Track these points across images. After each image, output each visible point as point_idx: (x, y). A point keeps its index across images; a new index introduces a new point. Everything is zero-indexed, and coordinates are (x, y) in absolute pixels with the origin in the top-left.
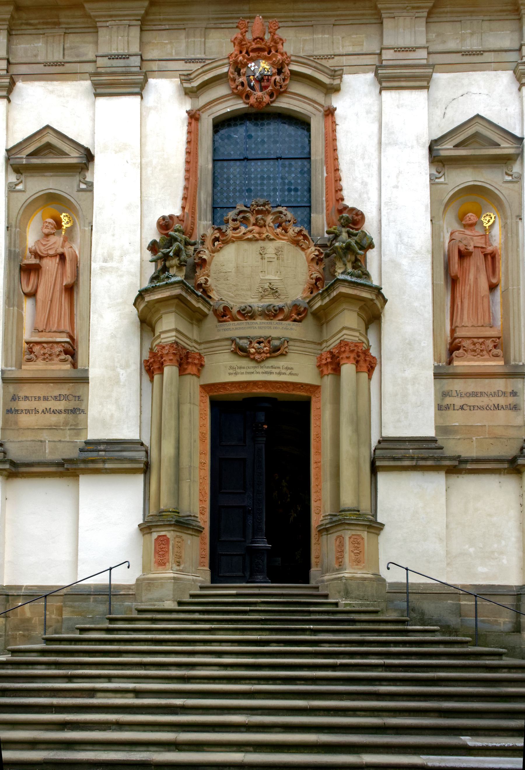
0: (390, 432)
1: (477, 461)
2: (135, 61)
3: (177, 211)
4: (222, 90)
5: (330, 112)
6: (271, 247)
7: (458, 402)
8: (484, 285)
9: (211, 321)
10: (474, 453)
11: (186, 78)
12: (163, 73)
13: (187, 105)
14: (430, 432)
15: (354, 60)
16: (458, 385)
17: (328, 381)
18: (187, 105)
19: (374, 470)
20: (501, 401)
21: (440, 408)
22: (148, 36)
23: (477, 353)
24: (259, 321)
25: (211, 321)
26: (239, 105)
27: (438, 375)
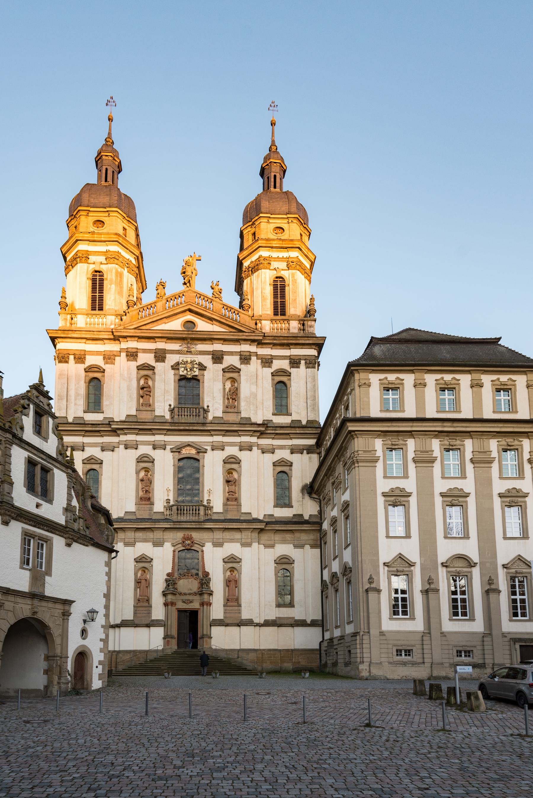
0: (214, 618)
1: (231, 624)
2: (162, 540)
3: (171, 571)
4: (180, 545)
5: (203, 551)
6: (190, 580)
7: (228, 612)
8: (234, 587)
9: (178, 595)
10: (231, 622)
11: (172, 544)
12: (168, 542)
13: (173, 548)
14: (222, 618)
15: (208, 540)
16: (228, 608)
17: (202, 608)
18: (173, 548)
19: (211, 626)
20: (237, 611)
21: (224, 613)
22: (164, 533)
23: (232, 602)
24: (188, 596)
25: (178, 595)
26: (184, 548)
27: (224, 606)
